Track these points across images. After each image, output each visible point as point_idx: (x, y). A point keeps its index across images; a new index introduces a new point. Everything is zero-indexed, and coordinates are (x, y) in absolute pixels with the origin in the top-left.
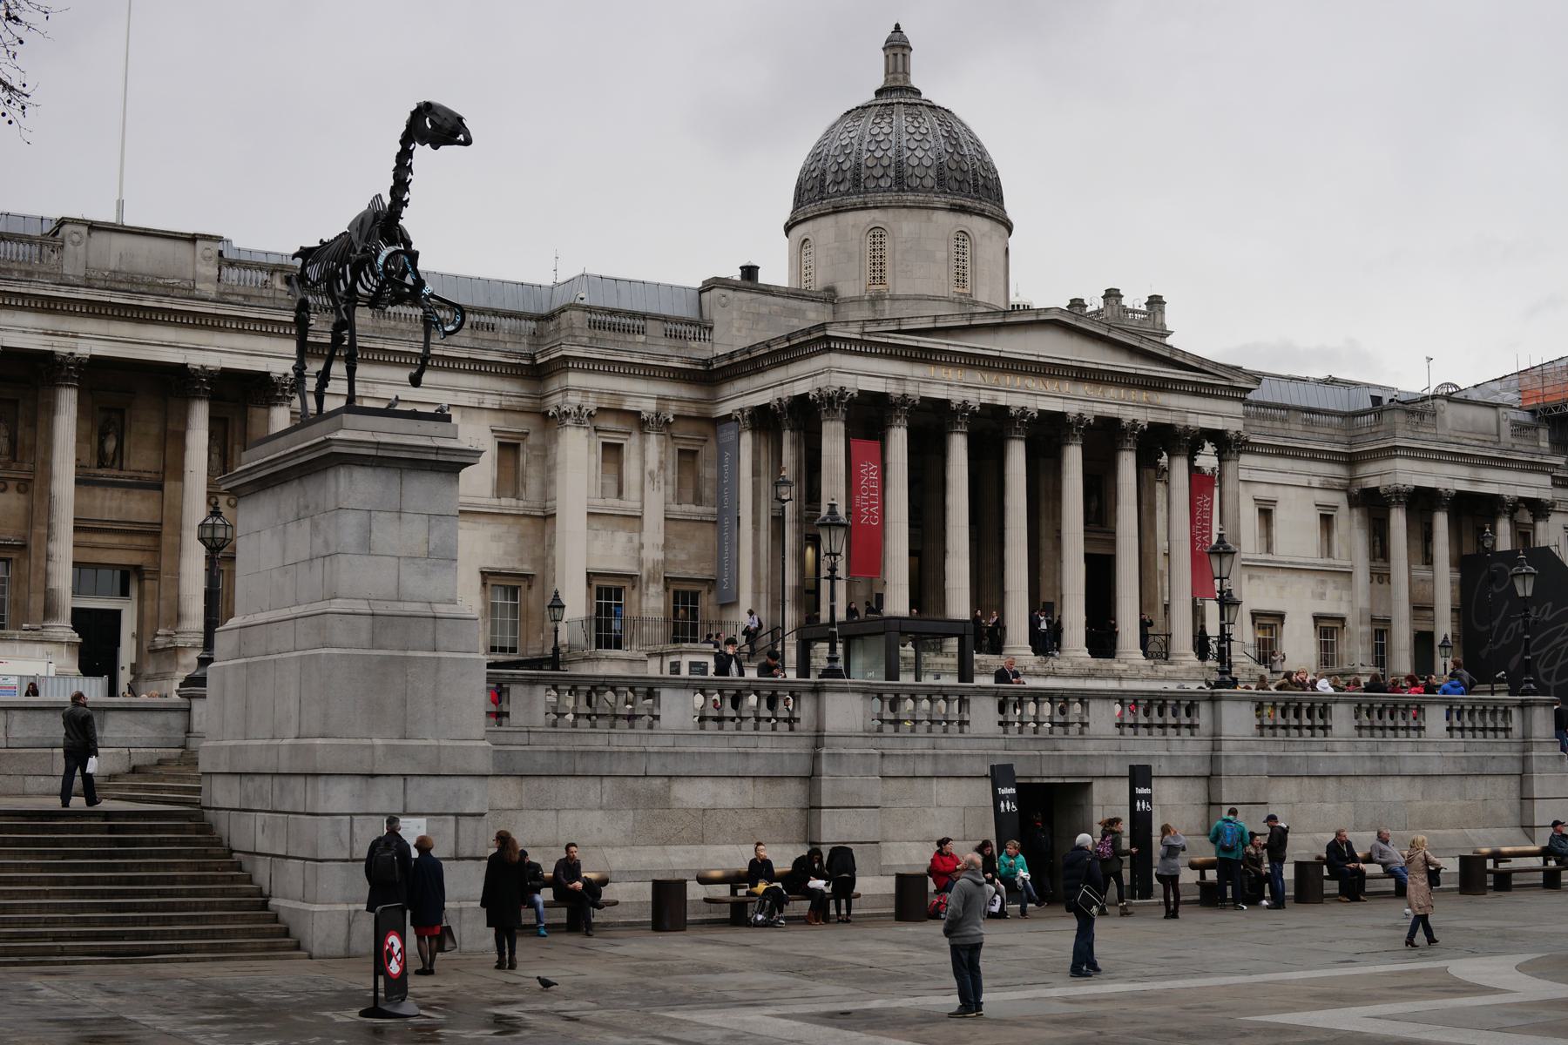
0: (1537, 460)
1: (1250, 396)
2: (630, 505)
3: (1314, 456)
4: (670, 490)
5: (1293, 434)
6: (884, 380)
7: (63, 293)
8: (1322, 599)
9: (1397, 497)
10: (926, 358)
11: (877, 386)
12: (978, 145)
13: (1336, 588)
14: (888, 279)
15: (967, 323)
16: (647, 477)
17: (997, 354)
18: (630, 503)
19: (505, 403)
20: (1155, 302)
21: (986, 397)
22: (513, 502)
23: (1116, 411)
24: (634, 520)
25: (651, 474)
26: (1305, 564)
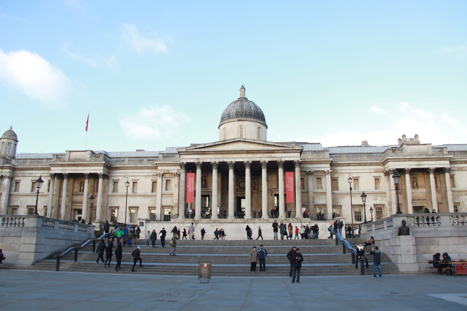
0: (441, 157)
2: (172, 192)
3: (371, 164)
5: (365, 160)
6: (194, 159)
7: (63, 163)
8: (376, 200)
9: (390, 172)
10: (204, 153)
11: (192, 161)
12: (256, 107)
13: (381, 197)
15: (214, 144)
17: (222, 150)
18: (171, 192)
20: (416, 136)
21: (221, 160)
26: (371, 192)
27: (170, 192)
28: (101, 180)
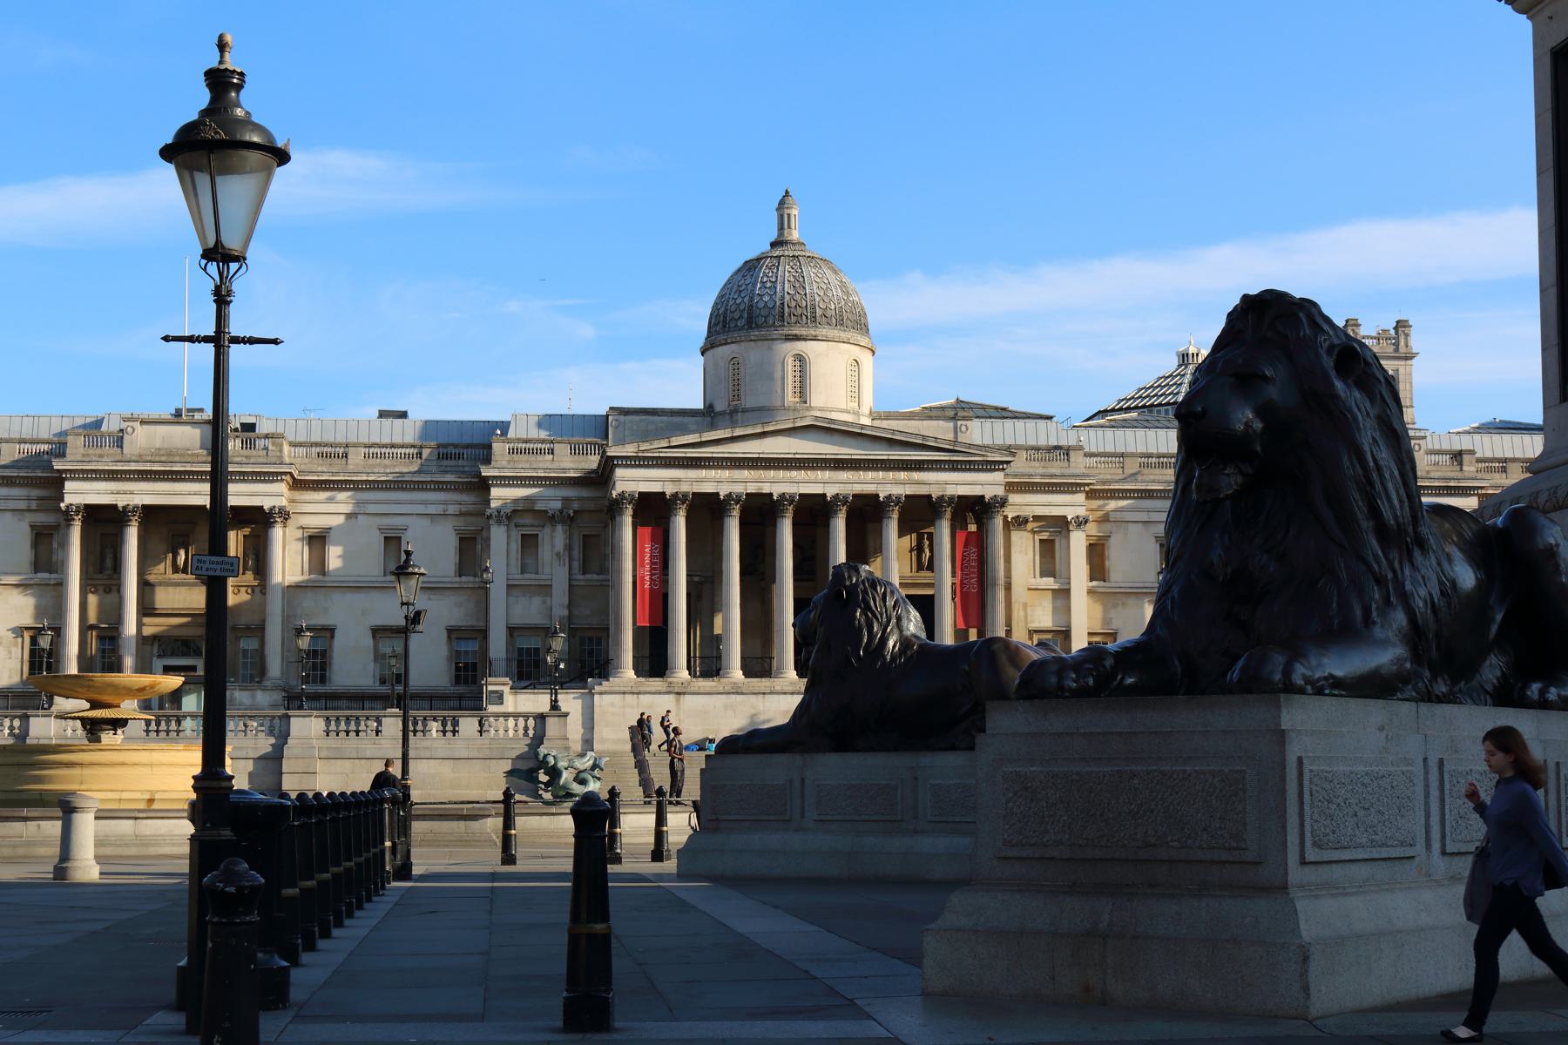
0: (1452, 484)
1: (1011, 469)
4: (576, 565)
6: (662, 483)
7: (119, 467)
11: (655, 488)
14: (743, 398)
15: (730, 435)
16: (555, 557)
17: (756, 456)
18: (543, 577)
19: (464, 509)
21: (752, 489)
22: (471, 579)
23: (873, 489)
24: (545, 589)
25: (558, 554)
27: (538, 576)
28: (277, 533)
